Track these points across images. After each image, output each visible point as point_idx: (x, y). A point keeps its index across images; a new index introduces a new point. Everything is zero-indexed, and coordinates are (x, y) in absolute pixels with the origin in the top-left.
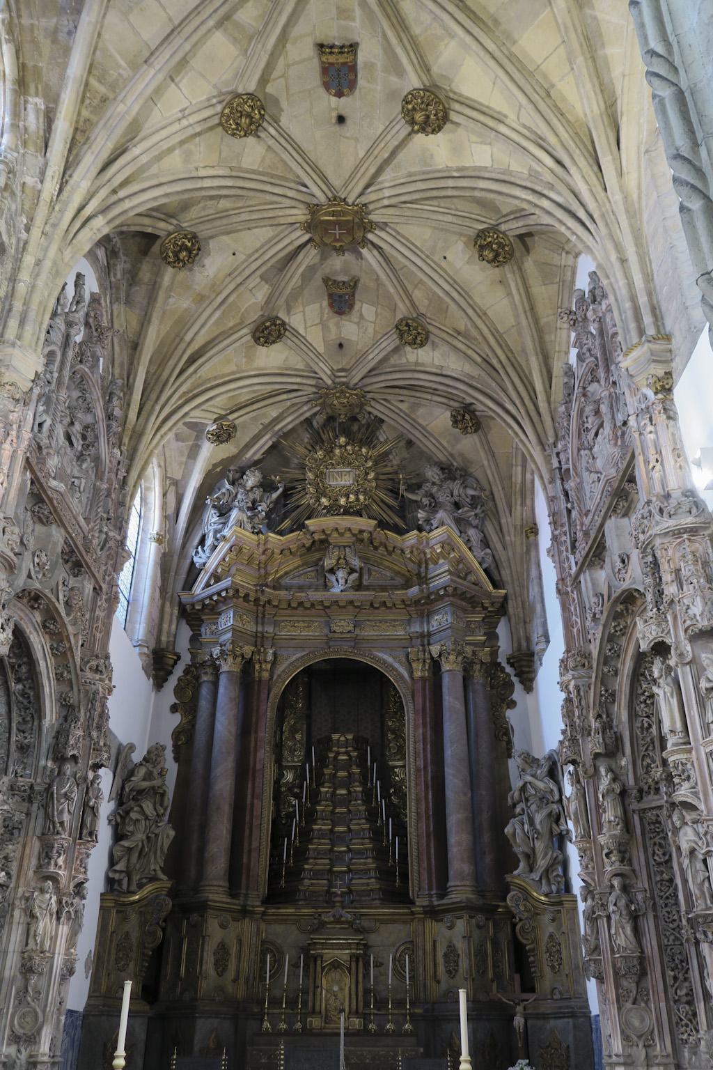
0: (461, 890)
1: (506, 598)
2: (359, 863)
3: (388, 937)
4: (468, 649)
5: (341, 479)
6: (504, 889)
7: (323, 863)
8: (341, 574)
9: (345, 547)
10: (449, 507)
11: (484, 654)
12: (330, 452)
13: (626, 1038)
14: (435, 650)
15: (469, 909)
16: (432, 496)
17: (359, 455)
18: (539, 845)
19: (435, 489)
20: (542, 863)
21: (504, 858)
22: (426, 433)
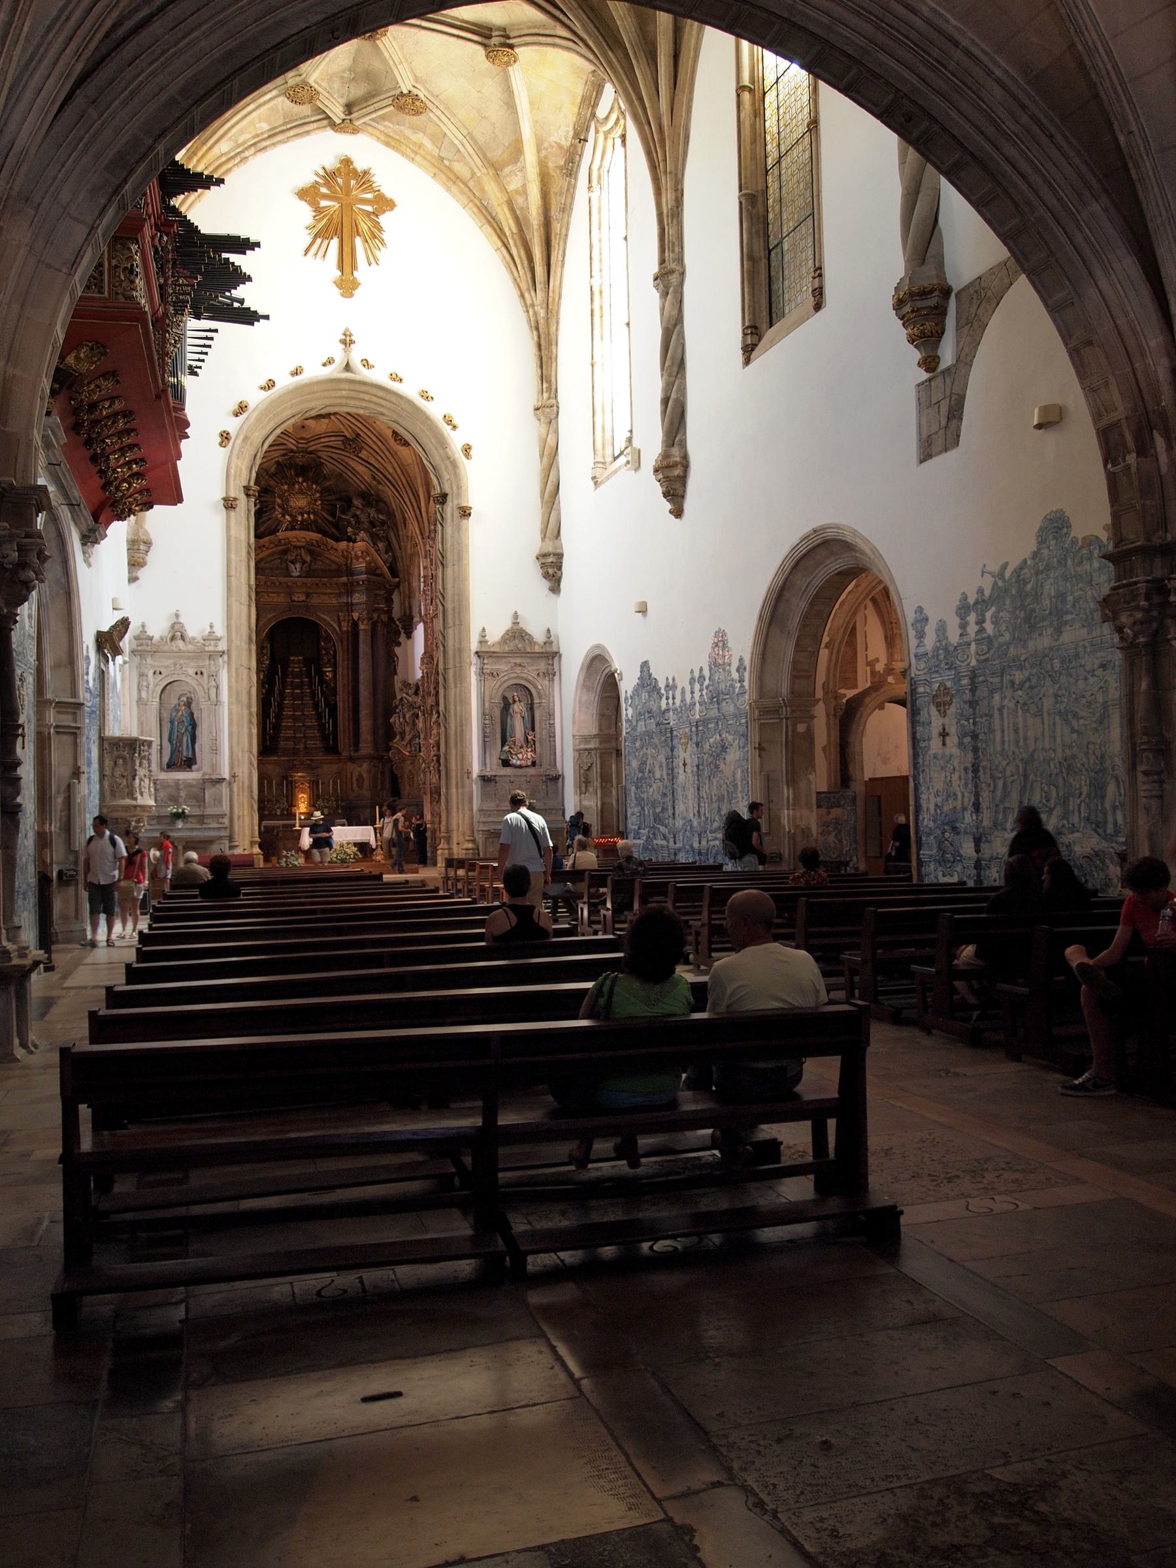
0: (366, 748)
1: (399, 582)
2: (310, 733)
3: (328, 769)
4: (375, 616)
5: (299, 502)
6: (389, 749)
7: (290, 733)
8: (298, 566)
9: (300, 547)
10: (366, 525)
11: (384, 618)
12: (291, 485)
13: (432, 815)
14: (356, 615)
15: (370, 758)
16: (356, 516)
17: (310, 488)
18: (407, 729)
19: (358, 513)
20: (408, 737)
21: (389, 733)
22: (354, 472)
